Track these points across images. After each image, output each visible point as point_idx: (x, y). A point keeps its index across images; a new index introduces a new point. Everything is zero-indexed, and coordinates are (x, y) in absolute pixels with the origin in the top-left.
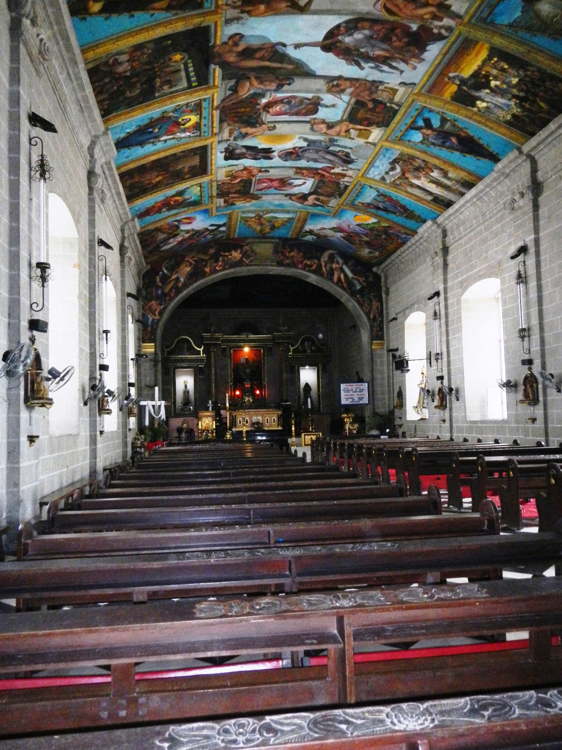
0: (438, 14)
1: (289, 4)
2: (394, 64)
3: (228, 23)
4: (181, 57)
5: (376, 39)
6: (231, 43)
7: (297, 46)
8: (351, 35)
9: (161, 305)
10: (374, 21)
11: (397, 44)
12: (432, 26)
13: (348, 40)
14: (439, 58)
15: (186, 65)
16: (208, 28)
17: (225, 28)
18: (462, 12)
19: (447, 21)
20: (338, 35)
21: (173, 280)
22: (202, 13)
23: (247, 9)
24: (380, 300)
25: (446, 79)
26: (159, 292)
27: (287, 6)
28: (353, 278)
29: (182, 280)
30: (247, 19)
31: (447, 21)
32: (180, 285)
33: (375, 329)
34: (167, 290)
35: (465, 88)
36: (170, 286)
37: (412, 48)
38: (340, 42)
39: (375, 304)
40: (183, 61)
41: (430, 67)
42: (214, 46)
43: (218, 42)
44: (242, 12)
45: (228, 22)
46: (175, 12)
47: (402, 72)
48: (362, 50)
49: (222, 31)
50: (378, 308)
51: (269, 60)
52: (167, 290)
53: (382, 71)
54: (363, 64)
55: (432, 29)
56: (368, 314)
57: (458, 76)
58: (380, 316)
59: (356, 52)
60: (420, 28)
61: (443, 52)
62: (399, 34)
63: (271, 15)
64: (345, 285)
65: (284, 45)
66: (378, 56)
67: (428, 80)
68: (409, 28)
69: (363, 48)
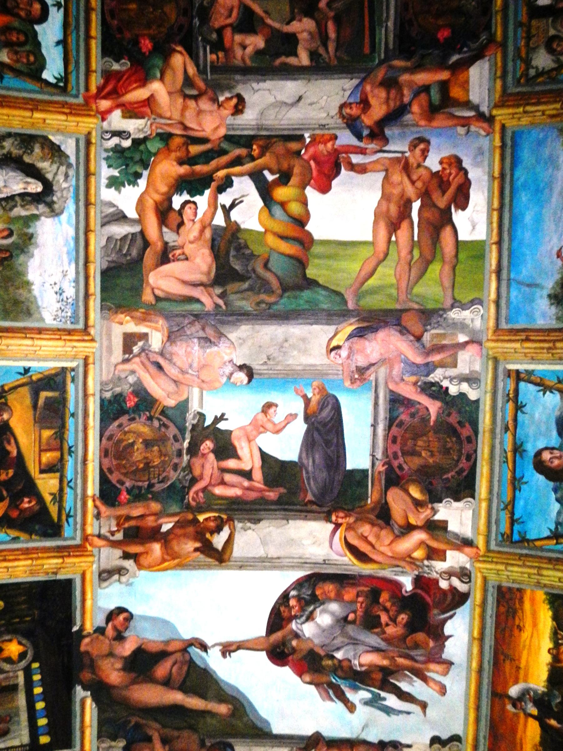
0: (434, 544)
1: (198, 545)
2: (404, 686)
3: (105, 580)
4: (21, 649)
5: (353, 622)
6: (110, 631)
7: (228, 649)
8: (310, 617)
10: (342, 580)
11: (391, 630)
12: (434, 575)
13: (308, 630)
14: (475, 650)
15: (28, 672)
16: (69, 583)
17: (100, 591)
18: (467, 531)
19: (455, 559)
20: (291, 619)
22: (59, 549)
23: (134, 549)
25: (509, 707)
27: (196, 550)
30: (135, 576)
31: (455, 559)
35: (553, 722)
37: (420, 636)
38: (297, 636)
40: (23, 664)
41: (468, 679)
42: (80, 634)
43: (89, 628)
44: (126, 556)
45: (106, 575)
46: (13, 533)
47: (424, 706)
48: (339, 655)
49: (94, 599)
51: (184, 688)
53: (388, 711)
54: (350, 695)
55: (437, 581)
57: (525, 693)
59: (330, 662)
60: (418, 581)
61: (476, 634)
62: (388, 605)
63: (174, 568)
65: (204, 647)
66: (373, 668)
67: (477, 720)
68: (398, 586)
69: (338, 649)
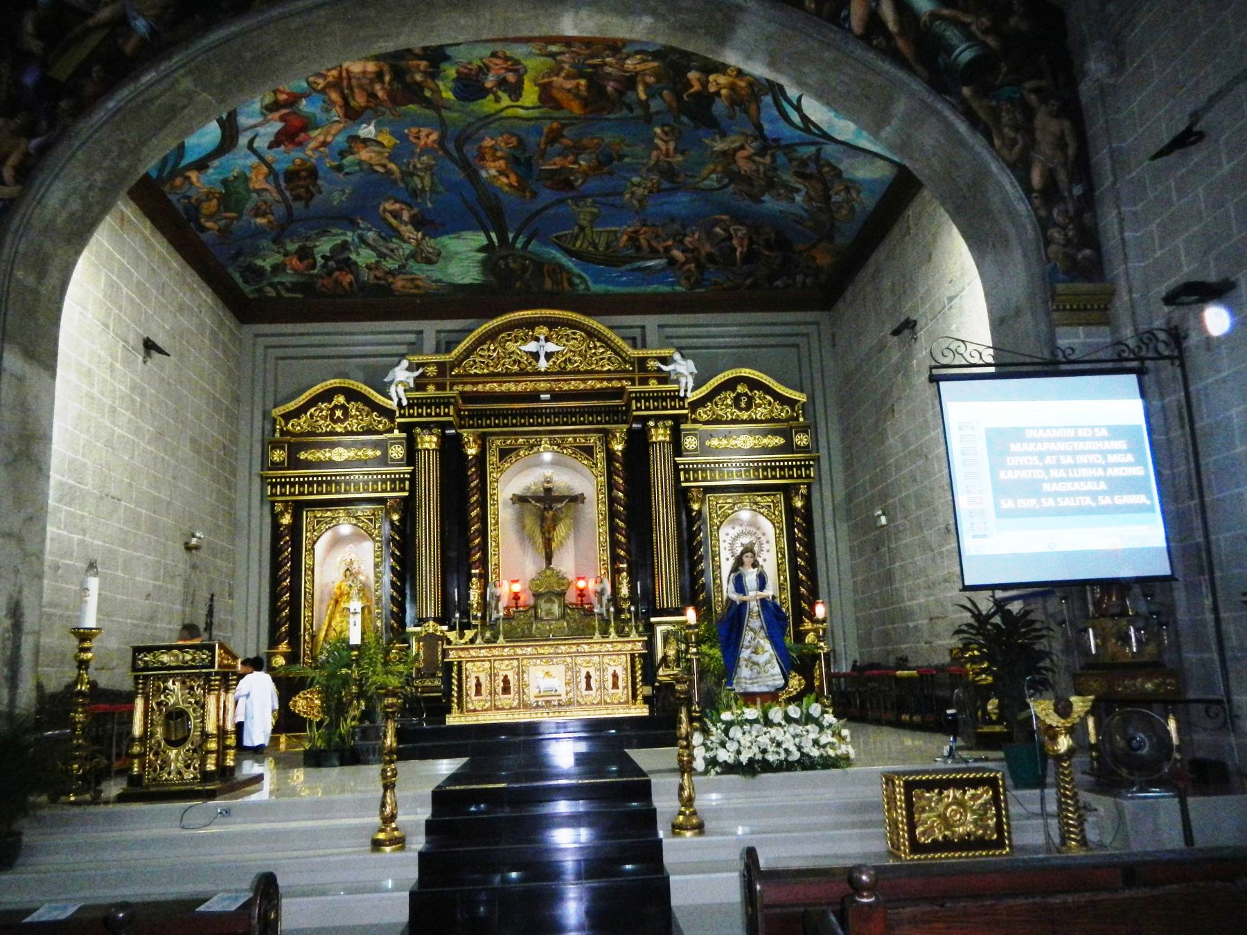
9: (30, 133)
21: (97, 27)
24: (1072, 111)
26: (29, 80)
28: (934, 16)
29: (141, 25)
32: (129, 47)
33: (1055, 233)
34: (63, 70)
36: (80, 53)
39: (1047, 126)
50: (1061, 144)
52: (63, 70)
56: (1020, 168)
58: (1072, 180)
64: (900, 43)
